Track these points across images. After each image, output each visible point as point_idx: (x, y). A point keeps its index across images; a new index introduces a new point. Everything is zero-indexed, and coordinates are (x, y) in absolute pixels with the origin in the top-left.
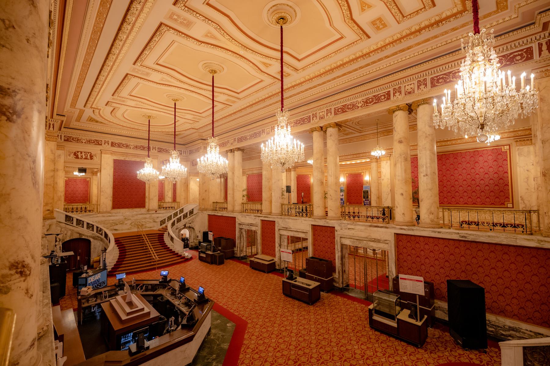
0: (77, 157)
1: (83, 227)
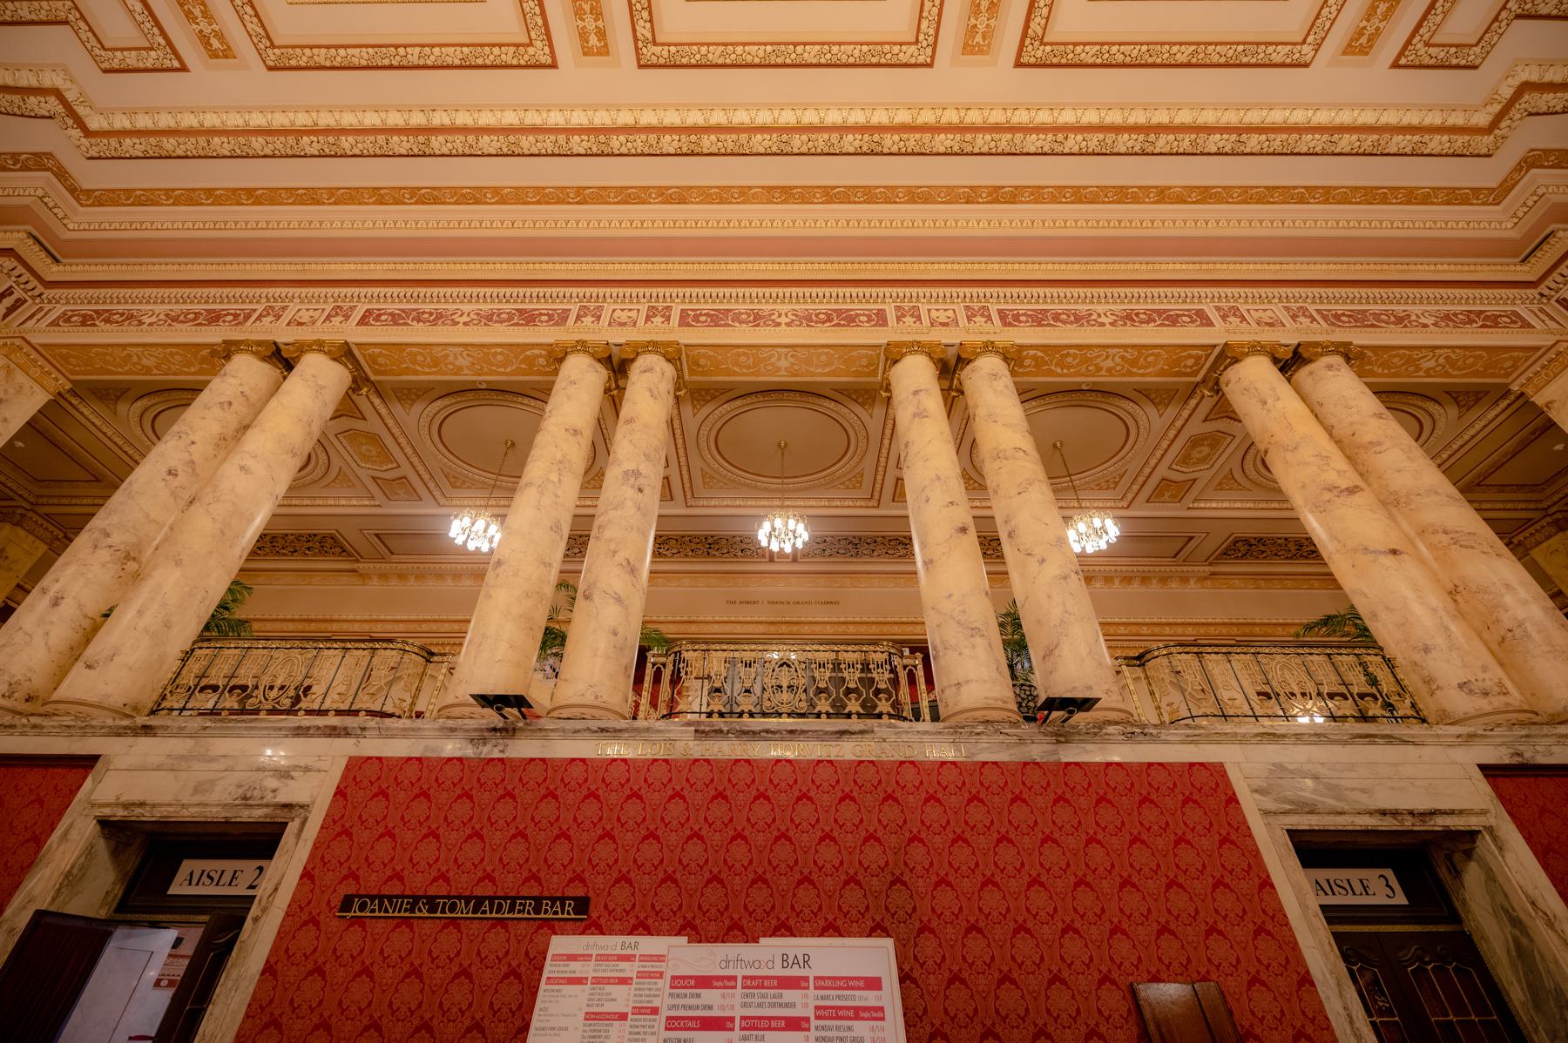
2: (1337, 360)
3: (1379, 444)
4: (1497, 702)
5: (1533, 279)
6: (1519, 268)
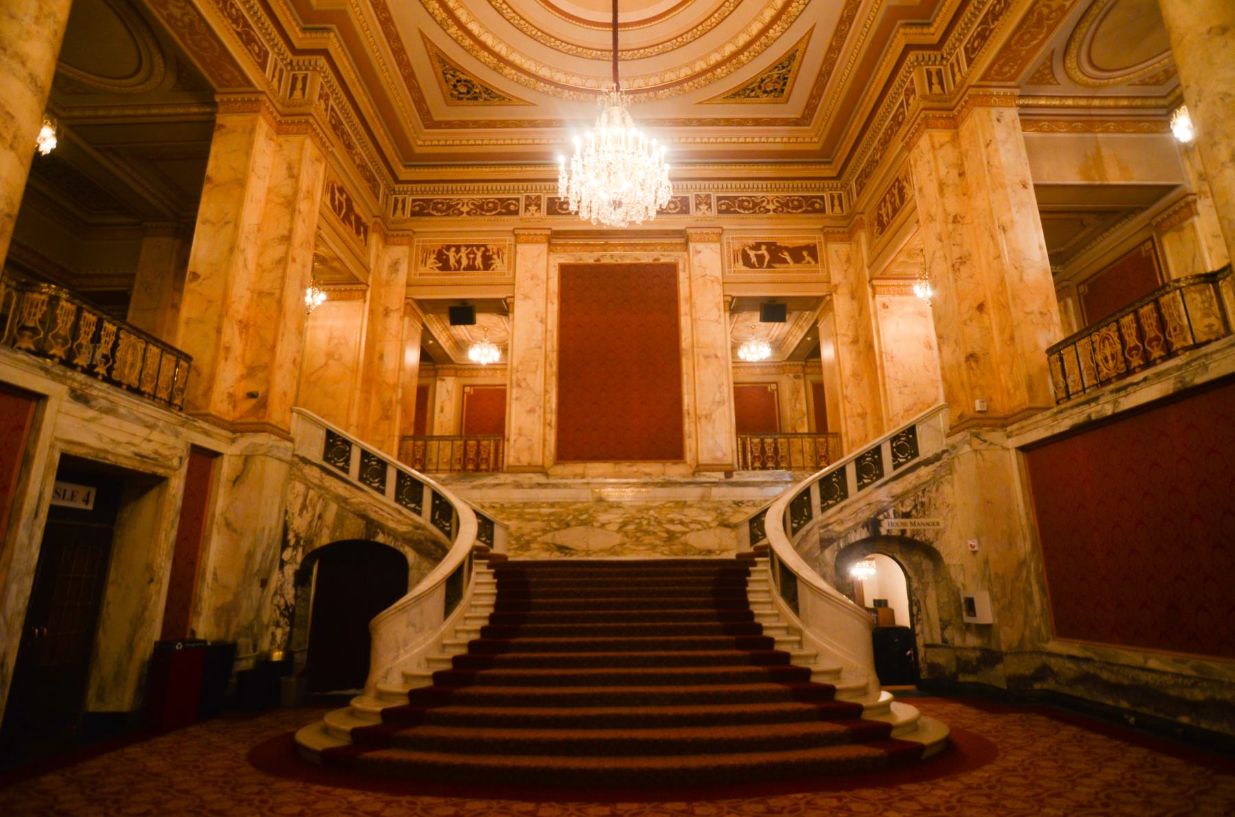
0: (445, 266)
1: (383, 492)
6: (297, 29)
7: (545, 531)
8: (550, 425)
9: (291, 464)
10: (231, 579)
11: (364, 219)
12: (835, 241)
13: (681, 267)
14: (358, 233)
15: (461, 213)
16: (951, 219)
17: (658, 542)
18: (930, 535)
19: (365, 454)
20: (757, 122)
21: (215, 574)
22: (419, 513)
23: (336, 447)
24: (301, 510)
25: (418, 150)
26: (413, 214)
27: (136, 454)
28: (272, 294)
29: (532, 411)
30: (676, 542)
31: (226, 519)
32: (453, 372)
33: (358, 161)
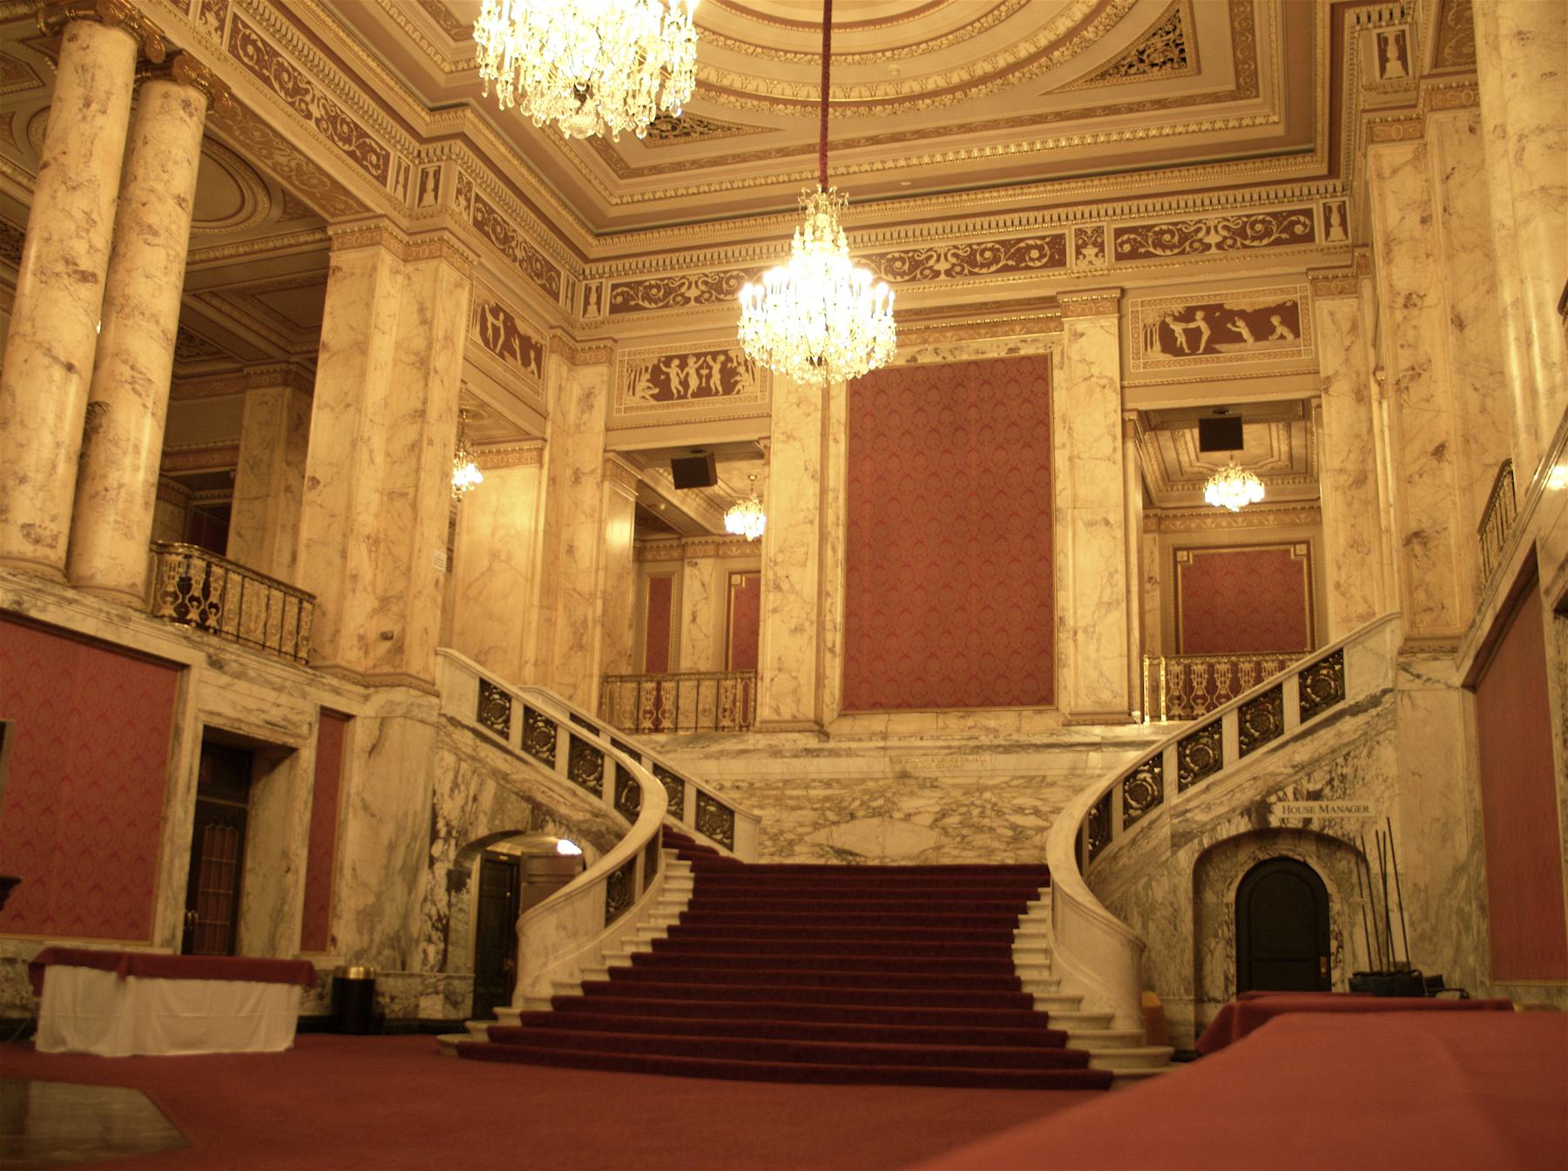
0: (664, 394)
1: (551, 764)
2: (198, 99)
3: (156, 234)
4: (41, 551)
5: (424, 134)
6: (423, 114)
7: (816, 826)
8: (832, 651)
9: (438, 727)
10: (372, 877)
11: (535, 338)
12: (1330, 294)
13: (1056, 360)
14: (526, 363)
15: (688, 300)
16: (1400, 300)
17: (996, 844)
18: (1351, 827)
19: (529, 712)
20: (1161, 104)
21: (354, 869)
22: (598, 793)
23: (492, 702)
24: (452, 790)
25: (613, 212)
26: (614, 309)
27: (268, 723)
28: (404, 495)
29: (798, 630)
30: (1027, 844)
31: (363, 800)
32: (711, 549)
33: (520, 254)
